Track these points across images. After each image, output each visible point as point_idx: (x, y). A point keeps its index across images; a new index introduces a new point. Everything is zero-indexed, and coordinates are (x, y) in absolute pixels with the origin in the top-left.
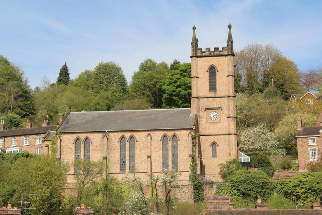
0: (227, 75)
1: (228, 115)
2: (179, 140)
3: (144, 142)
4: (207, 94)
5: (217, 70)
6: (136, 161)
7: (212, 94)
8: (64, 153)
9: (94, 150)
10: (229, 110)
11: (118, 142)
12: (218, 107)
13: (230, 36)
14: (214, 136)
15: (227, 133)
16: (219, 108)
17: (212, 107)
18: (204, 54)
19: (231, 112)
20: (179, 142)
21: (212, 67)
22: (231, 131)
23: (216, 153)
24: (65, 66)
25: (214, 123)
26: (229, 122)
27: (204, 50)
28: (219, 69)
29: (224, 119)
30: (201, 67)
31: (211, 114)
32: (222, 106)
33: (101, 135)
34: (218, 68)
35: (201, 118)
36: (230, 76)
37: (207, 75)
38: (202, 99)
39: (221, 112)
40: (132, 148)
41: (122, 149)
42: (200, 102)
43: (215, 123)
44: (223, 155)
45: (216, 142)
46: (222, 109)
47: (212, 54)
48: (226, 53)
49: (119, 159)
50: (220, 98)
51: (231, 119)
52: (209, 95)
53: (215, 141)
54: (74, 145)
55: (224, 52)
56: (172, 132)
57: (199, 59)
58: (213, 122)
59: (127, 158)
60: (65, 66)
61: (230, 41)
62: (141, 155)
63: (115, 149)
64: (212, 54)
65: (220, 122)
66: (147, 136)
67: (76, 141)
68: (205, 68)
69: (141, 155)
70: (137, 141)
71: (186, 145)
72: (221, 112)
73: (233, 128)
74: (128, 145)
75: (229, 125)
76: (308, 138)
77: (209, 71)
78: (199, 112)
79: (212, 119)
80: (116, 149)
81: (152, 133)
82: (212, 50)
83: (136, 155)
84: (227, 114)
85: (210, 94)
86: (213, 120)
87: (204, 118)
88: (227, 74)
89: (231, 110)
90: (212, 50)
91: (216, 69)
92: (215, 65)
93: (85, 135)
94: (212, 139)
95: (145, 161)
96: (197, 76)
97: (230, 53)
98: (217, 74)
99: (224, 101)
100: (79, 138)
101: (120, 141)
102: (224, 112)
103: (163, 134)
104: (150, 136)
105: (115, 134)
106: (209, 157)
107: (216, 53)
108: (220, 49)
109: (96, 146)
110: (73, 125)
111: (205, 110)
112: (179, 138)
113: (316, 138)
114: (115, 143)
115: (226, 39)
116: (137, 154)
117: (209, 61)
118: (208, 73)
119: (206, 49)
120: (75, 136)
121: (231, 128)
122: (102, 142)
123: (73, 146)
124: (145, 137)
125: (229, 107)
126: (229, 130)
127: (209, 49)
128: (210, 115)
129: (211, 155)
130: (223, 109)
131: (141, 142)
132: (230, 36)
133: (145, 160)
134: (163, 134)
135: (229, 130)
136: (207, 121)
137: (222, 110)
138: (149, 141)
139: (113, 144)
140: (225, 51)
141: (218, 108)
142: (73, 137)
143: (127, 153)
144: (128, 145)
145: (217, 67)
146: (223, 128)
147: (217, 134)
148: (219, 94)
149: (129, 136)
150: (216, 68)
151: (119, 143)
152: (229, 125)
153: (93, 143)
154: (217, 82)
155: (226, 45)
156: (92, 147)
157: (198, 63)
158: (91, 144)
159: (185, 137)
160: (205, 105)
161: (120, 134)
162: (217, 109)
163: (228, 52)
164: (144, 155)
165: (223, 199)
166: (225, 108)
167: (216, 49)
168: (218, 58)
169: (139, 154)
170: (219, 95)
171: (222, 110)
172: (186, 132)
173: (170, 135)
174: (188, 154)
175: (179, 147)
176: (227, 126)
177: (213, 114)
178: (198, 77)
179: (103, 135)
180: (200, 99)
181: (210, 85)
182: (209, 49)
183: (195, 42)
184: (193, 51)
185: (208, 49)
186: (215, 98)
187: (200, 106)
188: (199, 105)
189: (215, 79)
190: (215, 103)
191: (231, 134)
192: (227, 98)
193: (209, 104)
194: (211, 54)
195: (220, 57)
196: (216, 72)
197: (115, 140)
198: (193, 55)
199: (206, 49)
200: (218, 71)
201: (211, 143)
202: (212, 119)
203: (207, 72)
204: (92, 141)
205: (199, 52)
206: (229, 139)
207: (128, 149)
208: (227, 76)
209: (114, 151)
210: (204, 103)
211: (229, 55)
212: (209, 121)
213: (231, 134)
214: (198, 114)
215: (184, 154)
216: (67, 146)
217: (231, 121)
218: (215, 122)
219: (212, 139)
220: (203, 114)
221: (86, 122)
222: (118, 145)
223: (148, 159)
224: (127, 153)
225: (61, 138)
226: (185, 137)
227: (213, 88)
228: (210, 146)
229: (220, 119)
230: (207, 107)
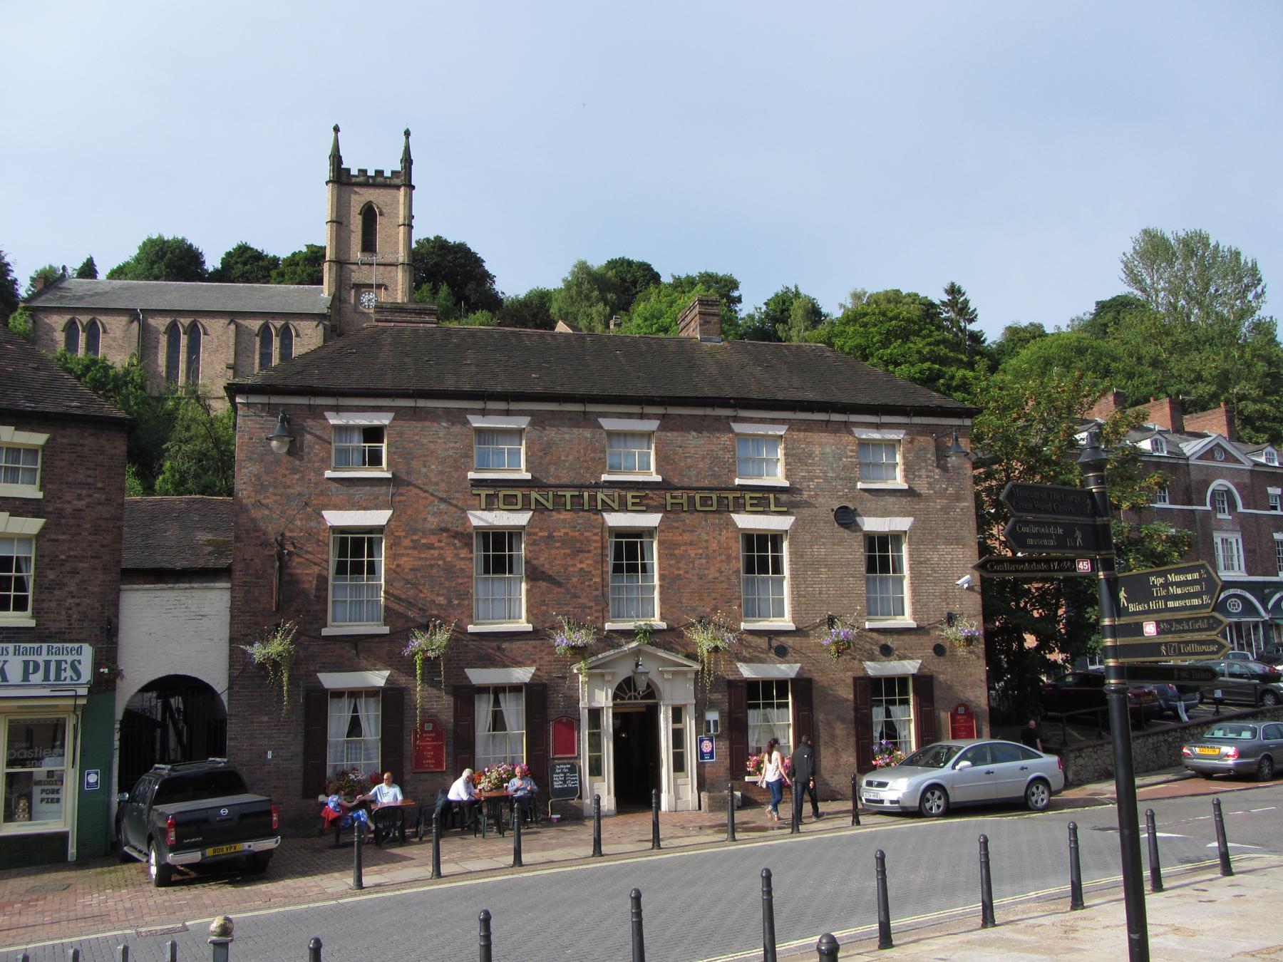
13: (407, 150)
16: (379, 286)
18: (354, 180)
27: (354, 172)
32: (387, 283)
40: (194, 348)
42: (342, 271)
47: (371, 181)
61: (407, 161)
62: (212, 361)
64: (371, 181)
69: (212, 361)
74: (184, 340)
78: (340, 291)
82: (371, 173)
90: (371, 173)
96: (339, 220)
107: (380, 180)
108: (388, 174)
109: (114, 339)
115: (400, 155)
118: (360, 217)
119: (360, 171)
120: (67, 317)
122: (127, 330)
132: (407, 150)
139: (153, 337)
143: (183, 357)
144: (184, 340)
155: (398, 167)
156: (103, 340)
165: (421, 313)
167: (379, 173)
171: (386, 289)
183: (336, 158)
188: (341, 276)
190: (374, 276)
194: (368, 181)
199: (359, 170)
221: (96, 294)
224: (183, 357)
227: (369, 245)
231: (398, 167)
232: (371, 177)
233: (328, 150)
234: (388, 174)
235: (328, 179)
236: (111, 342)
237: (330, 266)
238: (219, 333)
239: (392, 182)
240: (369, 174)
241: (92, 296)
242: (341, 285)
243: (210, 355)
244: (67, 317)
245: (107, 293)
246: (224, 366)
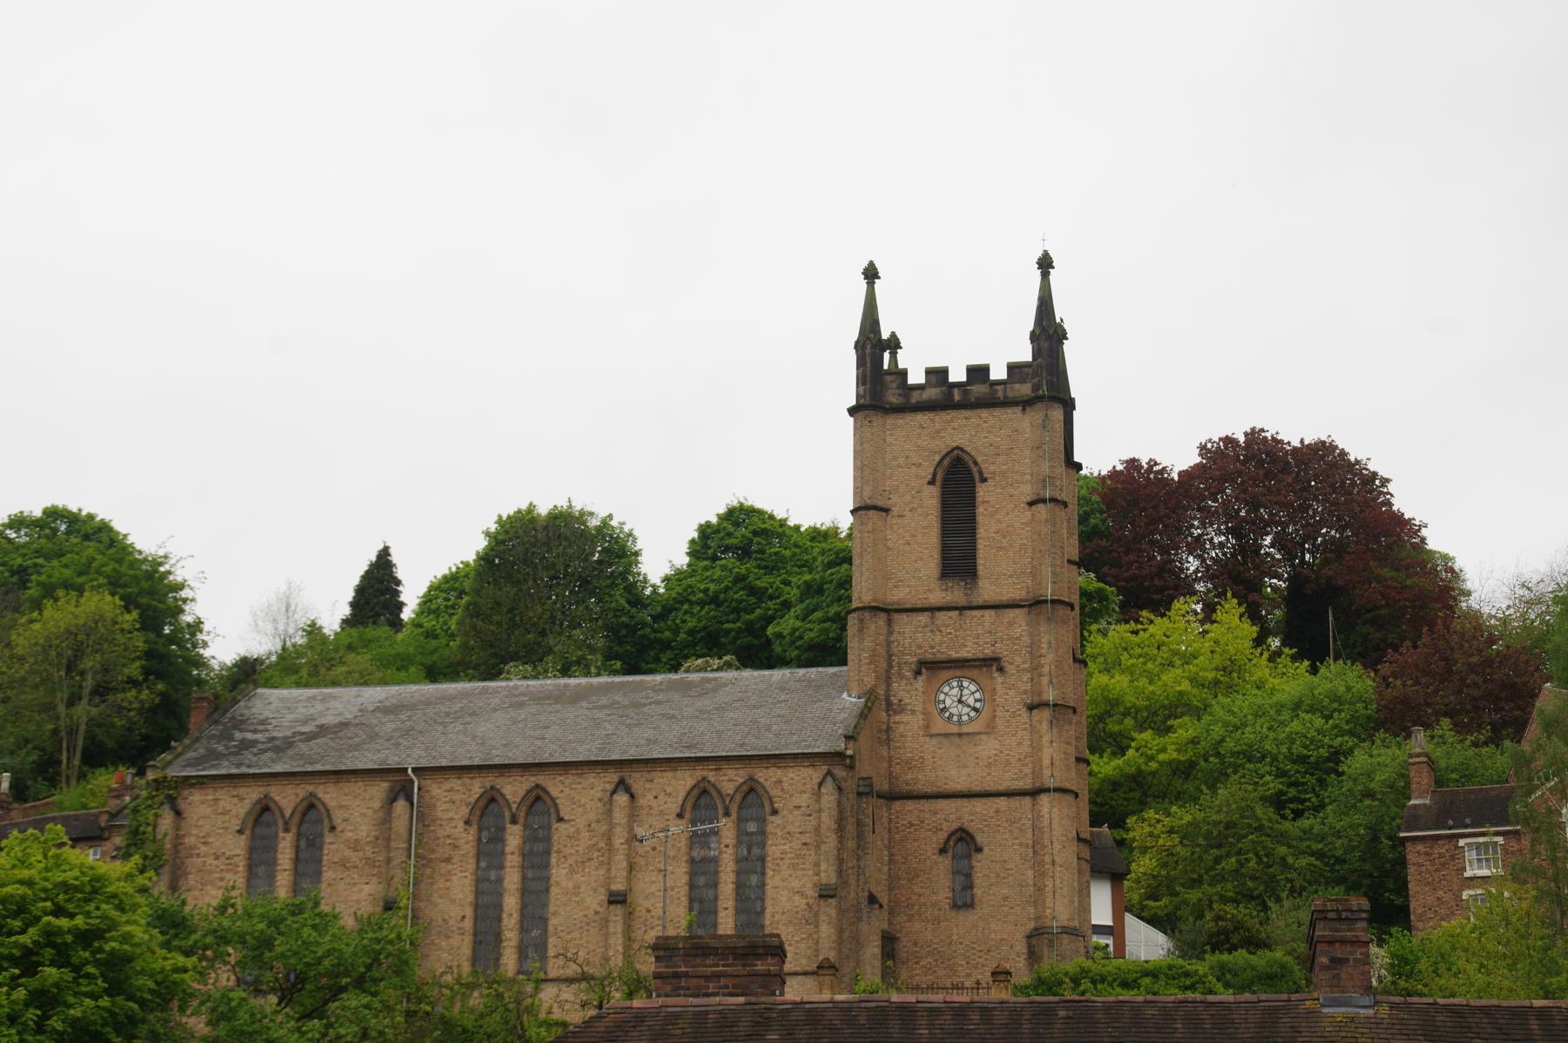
0: (1029, 499)
1: (1033, 693)
2: (775, 812)
3: (598, 821)
4: (930, 591)
5: (981, 473)
6: (553, 921)
7: (956, 595)
8: (192, 880)
9: (344, 864)
10: (1035, 669)
11: (467, 822)
12: (980, 656)
14: (959, 802)
15: (1026, 784)
16: (992, 663)
17: (954, 655)
18: (915, 397)
19: (1045, 680)
20: (773, 824)
21: (958, 459)
22: (1047, 772)
23: (969, 886)
24: (384, 556)
25: (960, 735)
26: (1033, 730)
27: (916, 377)
28: (992, 468)
29: (1014, 715)
30: (901, 461)
31: (946, 689)
32: (1001, 650)
33: (380, 789)
34: (982, 466)
35: (896, 713)
36: (1044, 501)
37: (931, 499)
38: (904, 616)
39: (1000, 680)
41: (489, 851)
42: (890, 633)
43: (968, 734)
44: (1006, 898)
45: (971, 830)
46: (1003, 664)
48: (1025, 390)
49: (469, 912)
50: (992, 612)
51: (1046, 714)
52: (938, 596)
53: (967, 825)
54: (243, 841)
55: (1017, 386)
56: (741, 772)
57: (891, 420)
58: (955, 729)
59: (511, 903)
60: (384, 556)
63: (448, 860)
65: (990, 728)
66: (614, 792)
67: (257, 822)
68: (919, 465)
70: (560, 820)
71: (807, 838)
74: (514, 838)
75: (1036, 747)
76: (1462, 843)
77: (939, 478)
79: (951, 715)
80: (456, 860)
81: (638, 781)
82: (957, 375)
83: (554, 890)
84: (1025, 692)
85: (946, 590)
86: (955, 718)
87: (913, 712)
88: (1027, 491)
89: (1046, 670)
90: (957, 375)
91: (975, 470)
92: (968, 449)
93: (303, 790)
94: (951, 814)
95: (597, 918)
96: (880, 503)
97: (1044, 391)
98: (982, 491)
99: (1010, 624)
100: (272, 805)
101: (475, 819)
102: (1011, 680)
103: (694, 782)
104: (628, 790)
105: (454, 783)
106: (934, 905)
107: (979, 389)
108: (998, 373)
109: (355, 846)
110: (246, 745)
111: (918, 673)
112: (772, 803)
113: (1500, 840)
114: (448, 830)
115: (1028, 323)
116: (558, 883)
117: (938, 432)
118: (934, 491)
120: (252, 794)
121: (1046, 762)
123: (237, 847)
124: (600, 800)
125: (1034, 654)
126: (1037, 773)
127: (944, 372)
128: (942, 697)
129: (944, 896)
130: (1010, 669)
131: (581, 822)
133: (597, 913)
134: (690, 782)
135: (1037, 773)
136: (927, 727)
137: (1001, 670)
138: (619, 816)
139: (441, 833)
140: (1022, 381)
141: (984, 660)
142: (241, 799)
143: (512, 879)
144: (514, 838)
145: (979, 460)
146: (1008, 763)
147: (977, 788)
148: (988, 589)
149: (522, 792)
150: (976, 463)
151: (473, 830)
152: (1036, 747)
153: (339, 829)
154: (981, 533)
155: (1025, 354)
156: (333, 849)
157: (889, 439)
158: (328, 838)
159: (804, 800)
160: (920, 647)
161: (477, 787)
162: (980, 667)
163: (1036, 388)
164: (595, 890)
166: (1017, 661)
167: (978, 373)
168: (985, 413)
169: (571, 885)
170: (986, 597)
171: (1001, 670)
172: (810, 771)
173: (728, 788)
174: (815, 885)
175: (774, 848)
176: (1026, 749)
177: (960, 696)
178: (887, 511)
179: (391, 789)
180: (896, 616)
181: (945, 550)
182: (944, 372)
184: (861, 380)
185: (937, 375)
186: (968, 612)
188: (889, 644)
189: (972, 519)
191: (1047, 790)
192: (1026, 609)
193: (938, 638)
194: (950, 395)
195: (997, 412)
196: (978, 484)
197: (451, 814)
198: (862, 401)
200: (984, 480)
201: (943, 836)
202: (951, 715)
203: (932, 482)
204: (337, 821)
205: (894, 385)
206: (1037, 817)
207: (512, 861)
208: (1031, 504)
209: (444, 867)
210: (914, 636)
211: (1040, 399)
212: (939, 726)
213: (1047, 790)
214: (881, 692)
215: (795, 884)
216: (205, 843)
217: (1045, 726)
218: (965, 729)
219: (951, 814)
220: (909, 691)
221: (323, 730)
222: (467, 839)
223: (612, 907)
224: (512, 879)
225: (182, 805)
226: (805, 796)
228: (943, 851)
229: (995, 716)
230: (929, 657)
231: (1025, 354)
232: (958, 385)
233: (852, 330)
234: (998, 373)
235: (853, 402)
236: (348, 853)
237: (861, 621)
238: (592, 816)
239: (1010, 394)
240: (951, 379)
241: (310, 737)
242: (890, 666)
243: (572, 871)
244: (252, 794)
245: (345, 725)
246: (603, 898)
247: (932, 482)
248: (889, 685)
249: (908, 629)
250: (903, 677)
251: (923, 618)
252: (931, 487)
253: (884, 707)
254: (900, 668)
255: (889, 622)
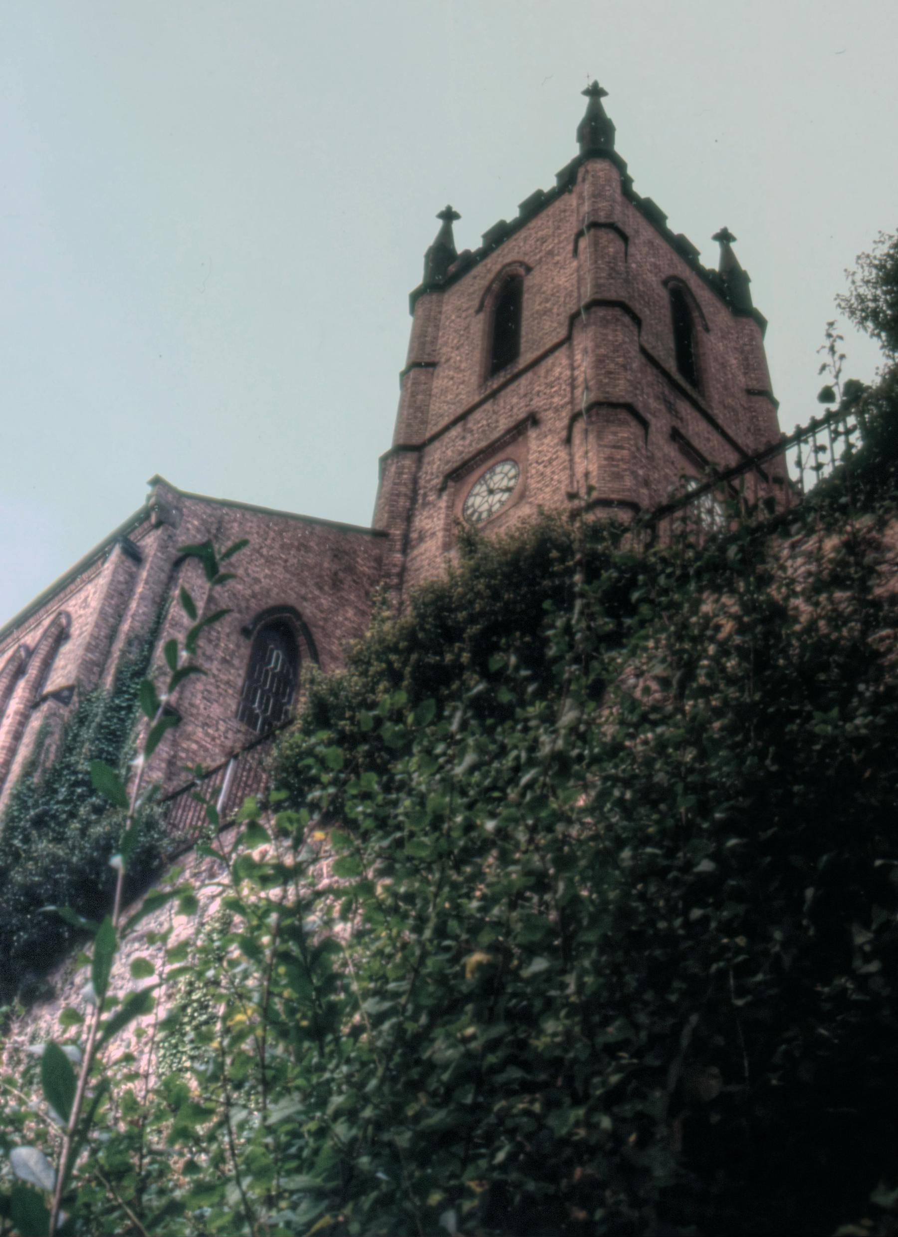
19: (578, 392)
32: (538, 403)
72: (532, 434)
73: (593, 468)
77: (489, 302)
99: (548, 372)
162: (514, 439)
187: (422, 482)
188: (415, 481)
193: (467, 442)
200: (529, 269)
214: (396, 533)
247: (480, 309)
248: (409, 518)
249: (437, 455)
250: (425, 504)
251: (454, 432)
252: (481, 316)
253: (398, 546)
254: (425, 495)
255: (419, 462)
